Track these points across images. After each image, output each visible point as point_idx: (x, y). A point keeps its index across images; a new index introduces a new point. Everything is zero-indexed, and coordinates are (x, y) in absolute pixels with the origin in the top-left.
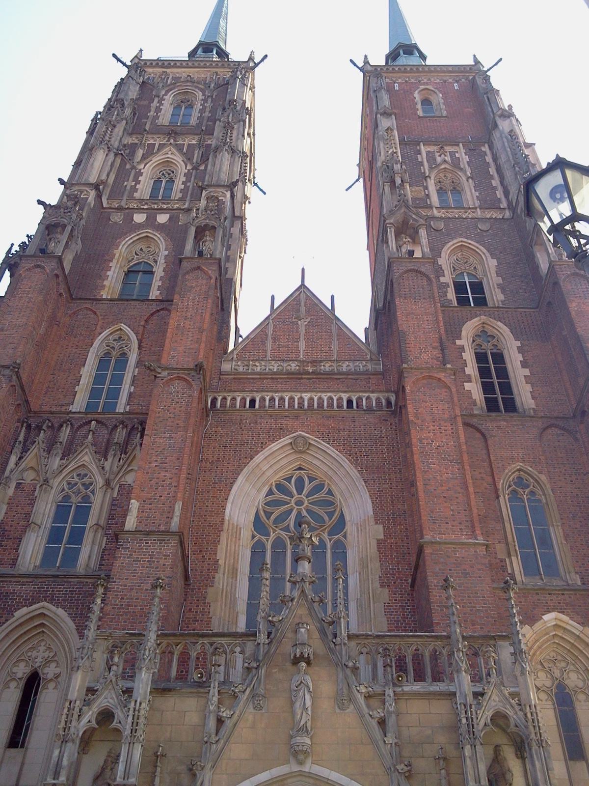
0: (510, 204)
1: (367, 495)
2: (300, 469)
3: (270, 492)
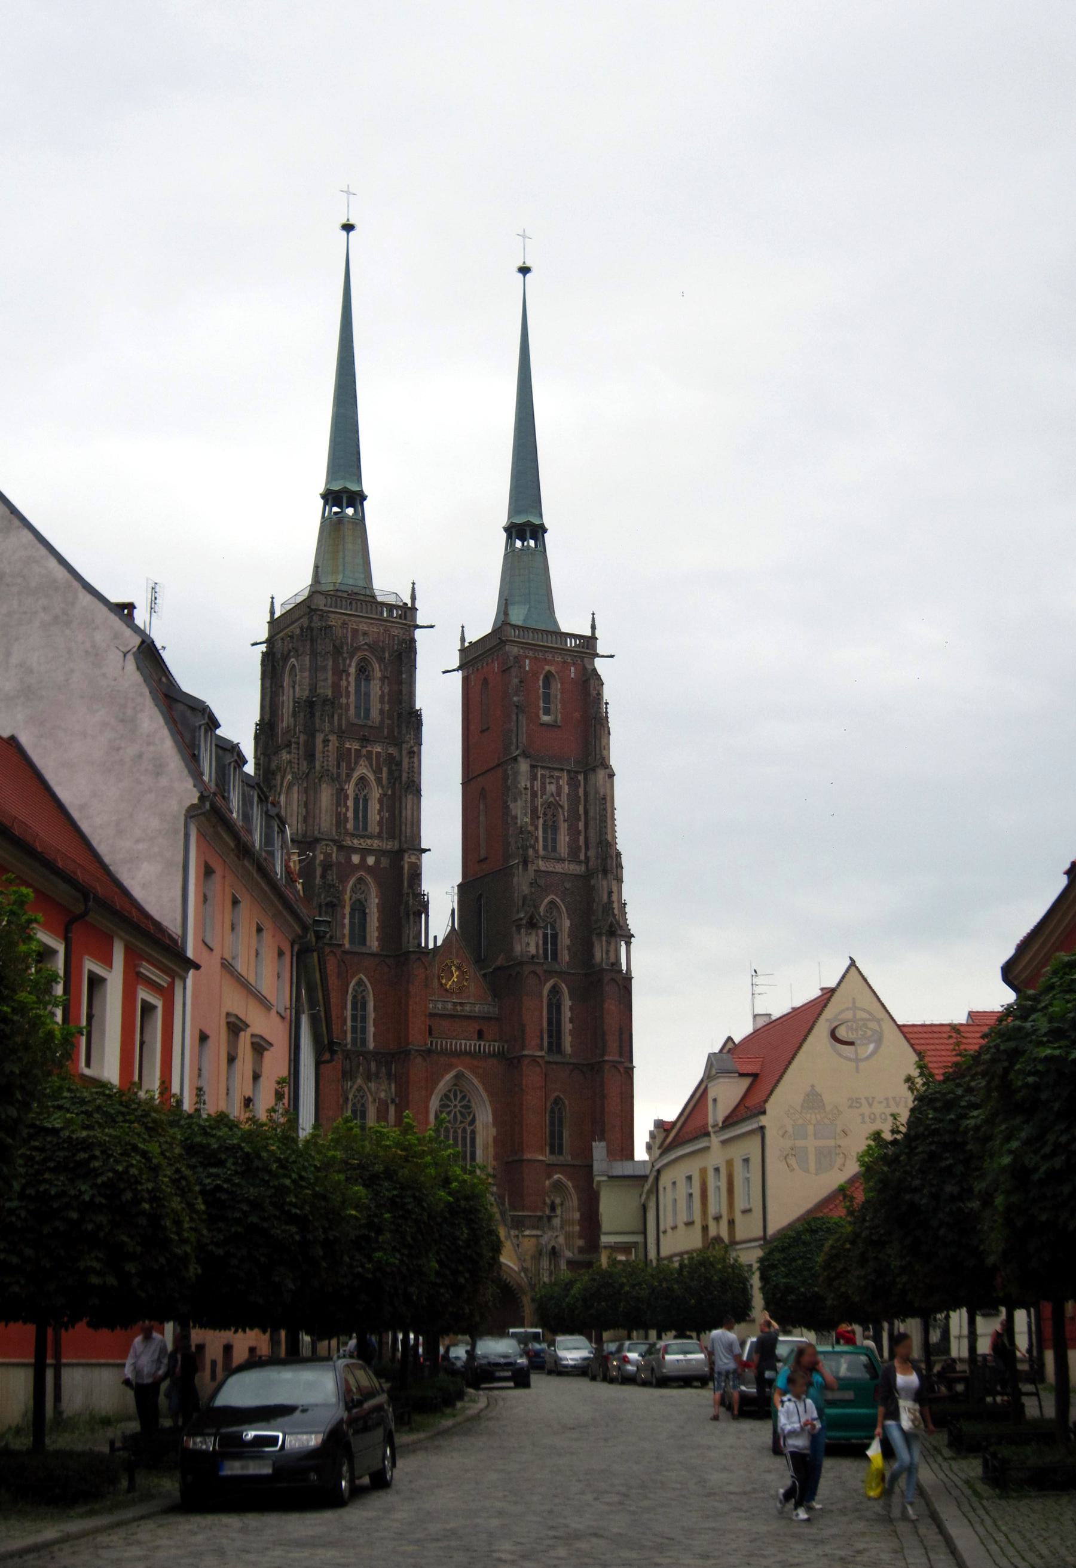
0: (587, 857)
1: (490, 1111)
2: (455, 1085)
3: (441, 1100)
